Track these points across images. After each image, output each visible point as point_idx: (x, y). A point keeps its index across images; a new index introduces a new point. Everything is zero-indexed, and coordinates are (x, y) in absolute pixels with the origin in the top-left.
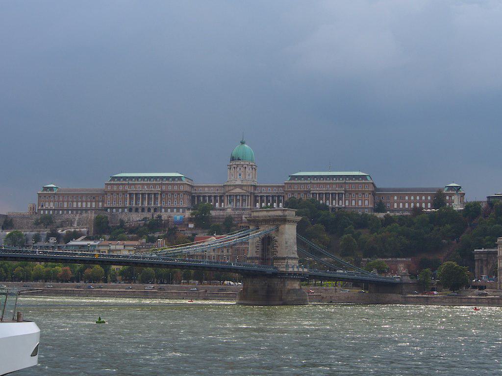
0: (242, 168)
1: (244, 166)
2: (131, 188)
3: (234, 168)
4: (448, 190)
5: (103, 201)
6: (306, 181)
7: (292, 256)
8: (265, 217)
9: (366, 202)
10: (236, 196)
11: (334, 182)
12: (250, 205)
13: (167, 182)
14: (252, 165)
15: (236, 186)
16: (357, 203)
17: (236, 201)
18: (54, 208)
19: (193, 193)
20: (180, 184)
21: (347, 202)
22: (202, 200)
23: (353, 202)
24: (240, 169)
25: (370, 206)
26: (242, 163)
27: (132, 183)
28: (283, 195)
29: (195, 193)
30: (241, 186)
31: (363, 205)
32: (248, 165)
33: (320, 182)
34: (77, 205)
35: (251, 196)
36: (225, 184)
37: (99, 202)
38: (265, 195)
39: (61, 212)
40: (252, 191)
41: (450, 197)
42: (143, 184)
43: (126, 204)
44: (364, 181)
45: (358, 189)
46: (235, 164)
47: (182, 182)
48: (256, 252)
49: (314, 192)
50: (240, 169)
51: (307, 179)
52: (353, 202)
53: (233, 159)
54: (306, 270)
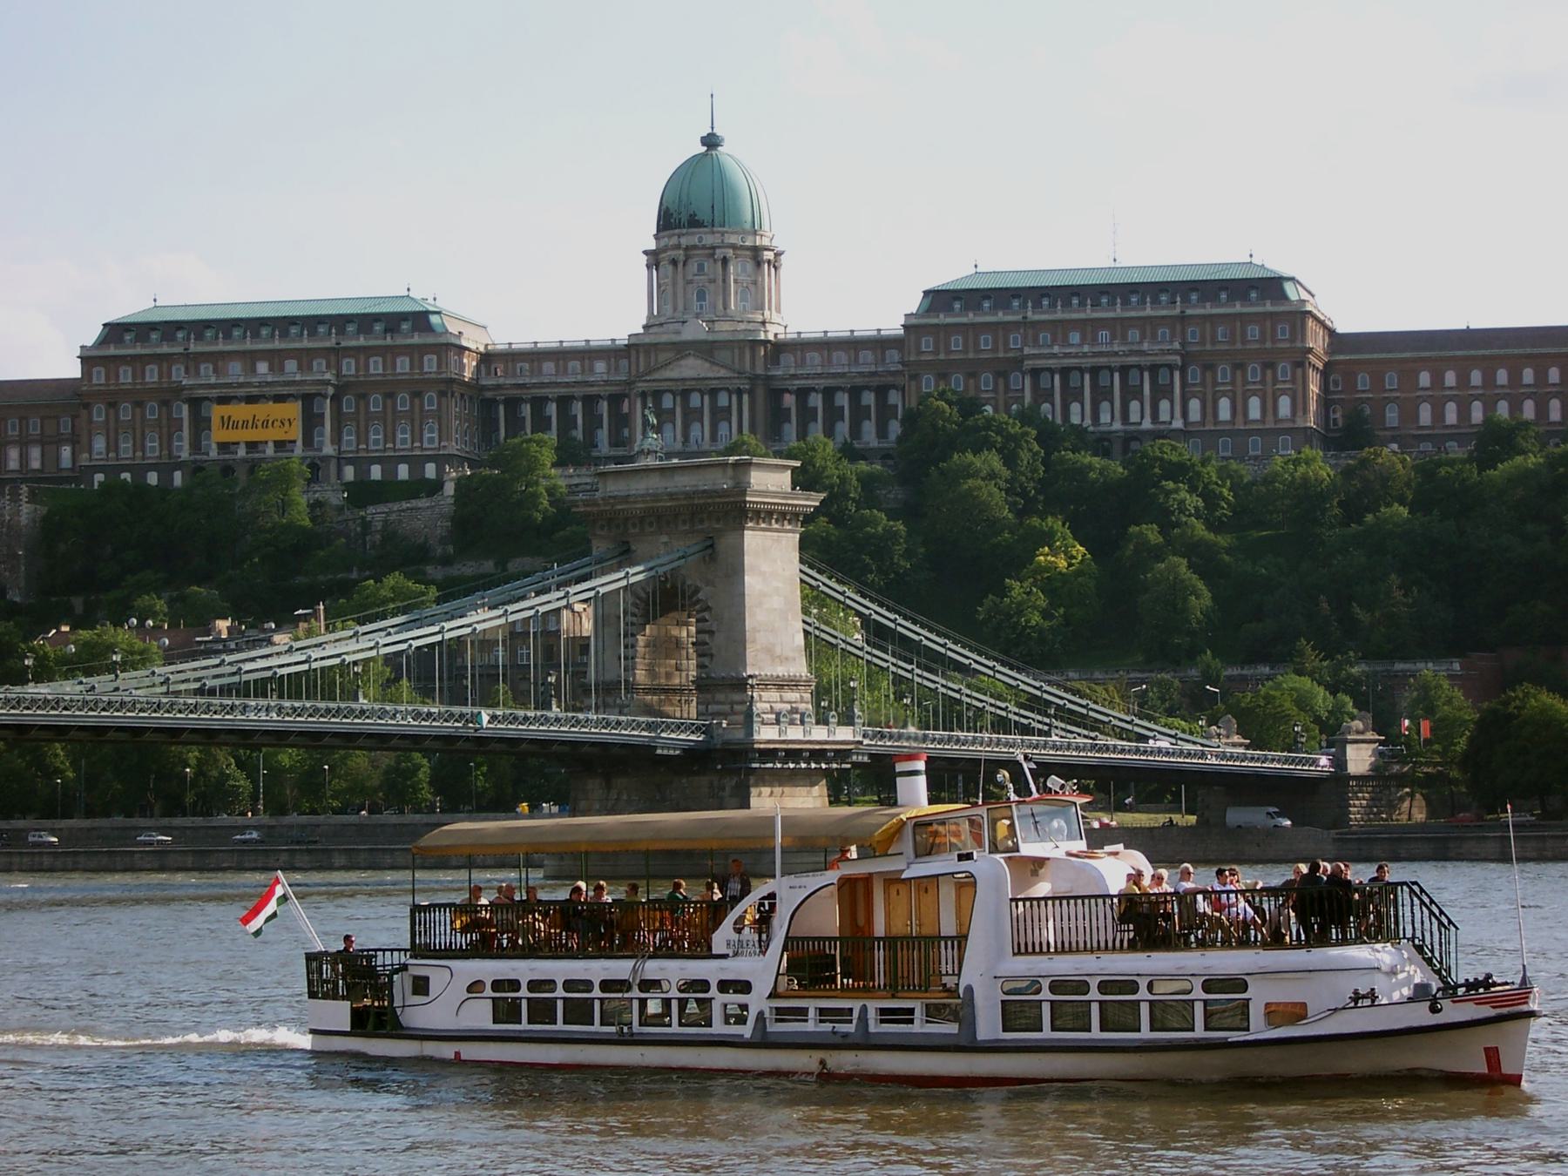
2: (198, 373)
3: (674, 262)
5: (74, 441)
6: (1001, 316)
7: (781, 671)
8: (656, 497)
11: (1133, 314)
15: (682, 349)
16: (1239, 408)
17: (685, 415)
19: (484, 388)
20: (424, 349)
21: (1195, 405)
23: (1224, 405)
24: (701, 268)
25: (1300, 423)
26: (709, 240)
27: (200, 349)
28: (900, 381)
29: (499, 387)
30: (706, 349)
31: (1270, 417)
32: (734, 247)
33: (1067, 316)
35: (751, 392)
37: (59, 441)
40: (760, 371)
42: (251, 358)
43: (180, 448)
44: (1269, 307)
46: (678, 247)
47: (430, 340)
50: (701, 268)
51: (1007, 307)
52: (1224, 405)
54: (844, 734)
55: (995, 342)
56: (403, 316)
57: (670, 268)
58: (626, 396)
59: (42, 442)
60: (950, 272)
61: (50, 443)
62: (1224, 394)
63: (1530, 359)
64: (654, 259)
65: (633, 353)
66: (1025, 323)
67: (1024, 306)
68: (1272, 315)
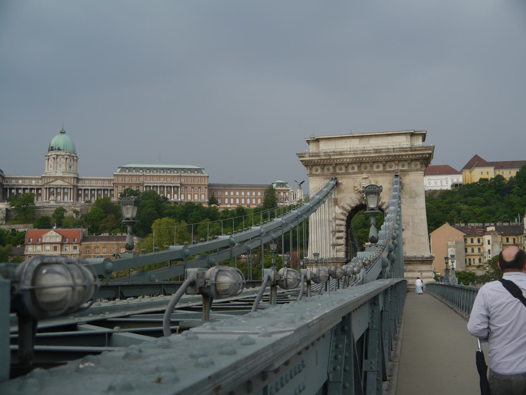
1: (65, 157)
3: (54, 158)
4: (276, 186)
6: (137, 174)
8: (363, 152)
9: (203, 196)
10: (57, 188)
12: (73, 199)
14: (73, 157)
15: (56, 178)
22: (15, 194)
26: (63, 153)
29: (8, 185)
30: (62, 178)
35: (73, 189)
36: (43, 175)
38: (90, 188)
40: (75, 184)
41: (285, 193)
44: (200, 175)
48: (334, 245)
49: (148, 185)
50: (60, 160)
52: (189, 196)
53: (52, 149)
57: (53, 160)
58: (40, 189)
65: (43, 179)
66: (144, 175)
67: (143, 171)
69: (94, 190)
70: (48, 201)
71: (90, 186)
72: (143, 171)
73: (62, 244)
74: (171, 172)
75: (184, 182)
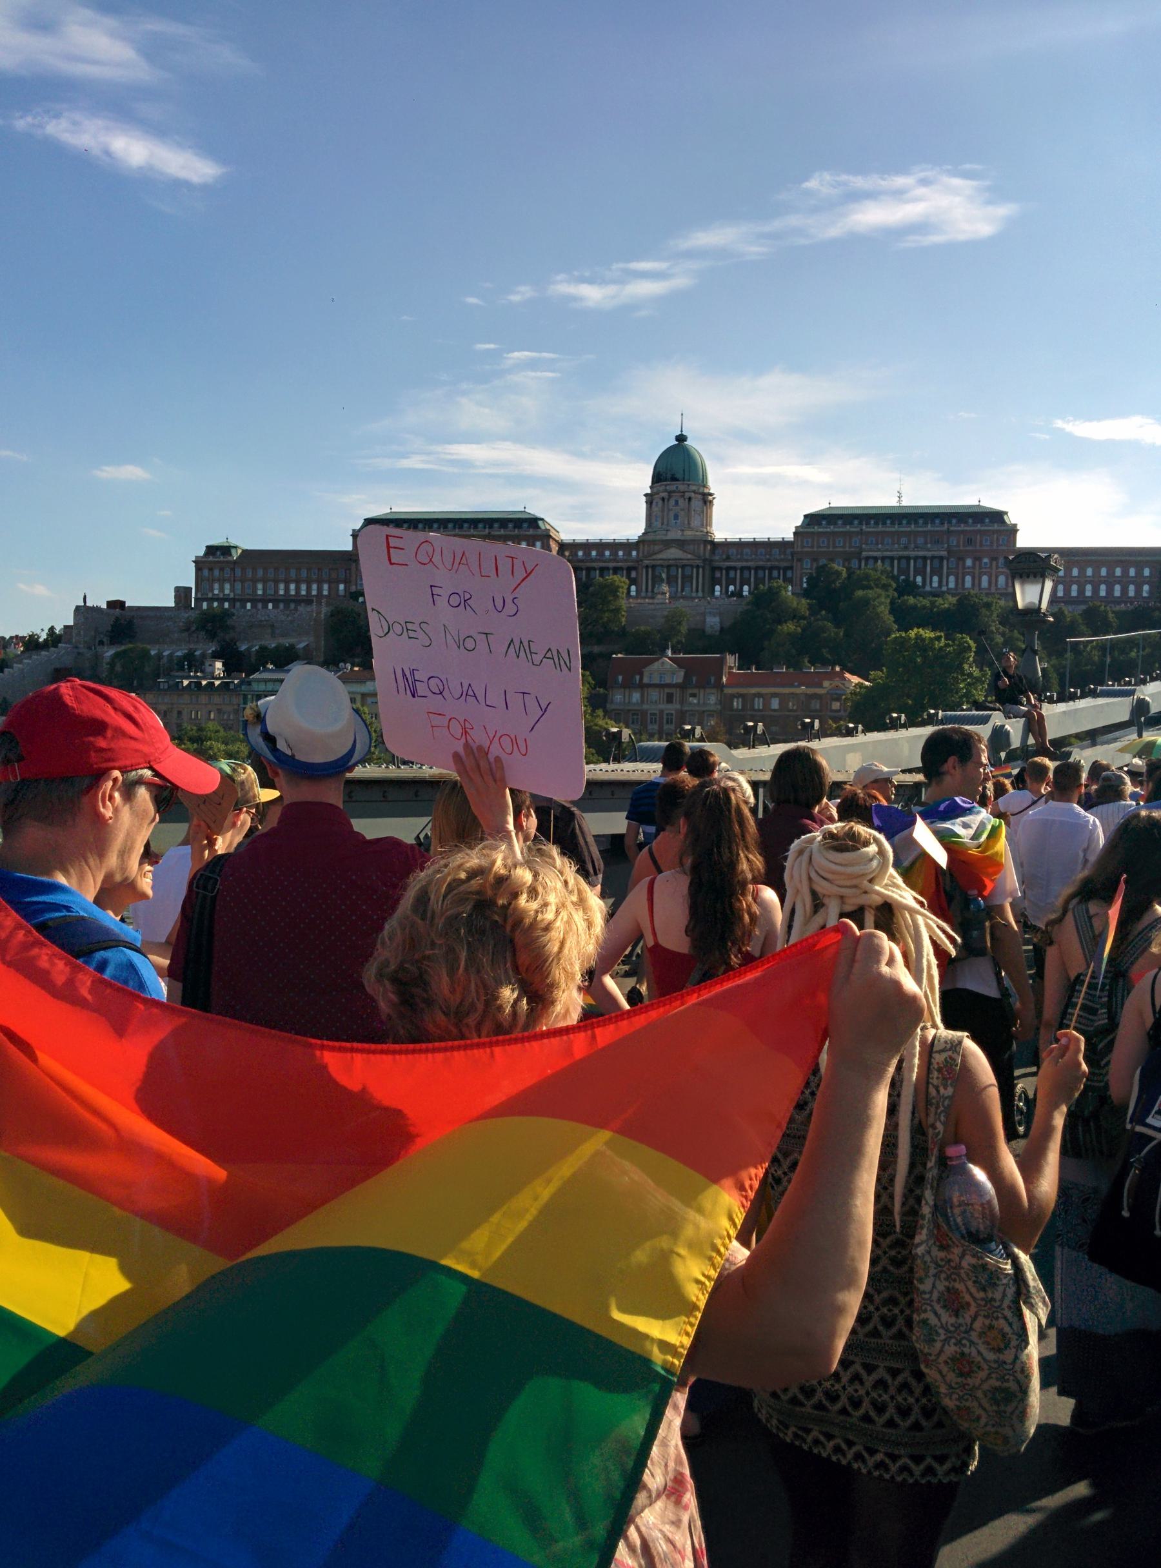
0: (681, 501)
1: (687, 495)
3: (663, 499)
12: (703, 591)
13: (502, 532)
15: (668, 544)
18: (232, 596)
24: (677, 503)
26: (682, 488)
30: (681, 544)
32: (694, 492)
34: (287, 589)
37: (339, 582)
38: (739, 564)
39: (249, 606)
40: (707, 556)
45: (981, 545)
50: (677, 503)
55: (845, 543)
56: (525, 520)
58: (634, 568)
59: (329, 582)
60: (818, 505)
61: (333, 583)
62: (968, 574)
63: (1119, 563)
64: (650, 499)
66: (861, 532)
68: (998, 531)
69: (749, 568)
70: (650, 594)
71: (739, 560)
72: (861, 523)
73: (682, 687)
74: (926, 523)
75: (958, 545)
